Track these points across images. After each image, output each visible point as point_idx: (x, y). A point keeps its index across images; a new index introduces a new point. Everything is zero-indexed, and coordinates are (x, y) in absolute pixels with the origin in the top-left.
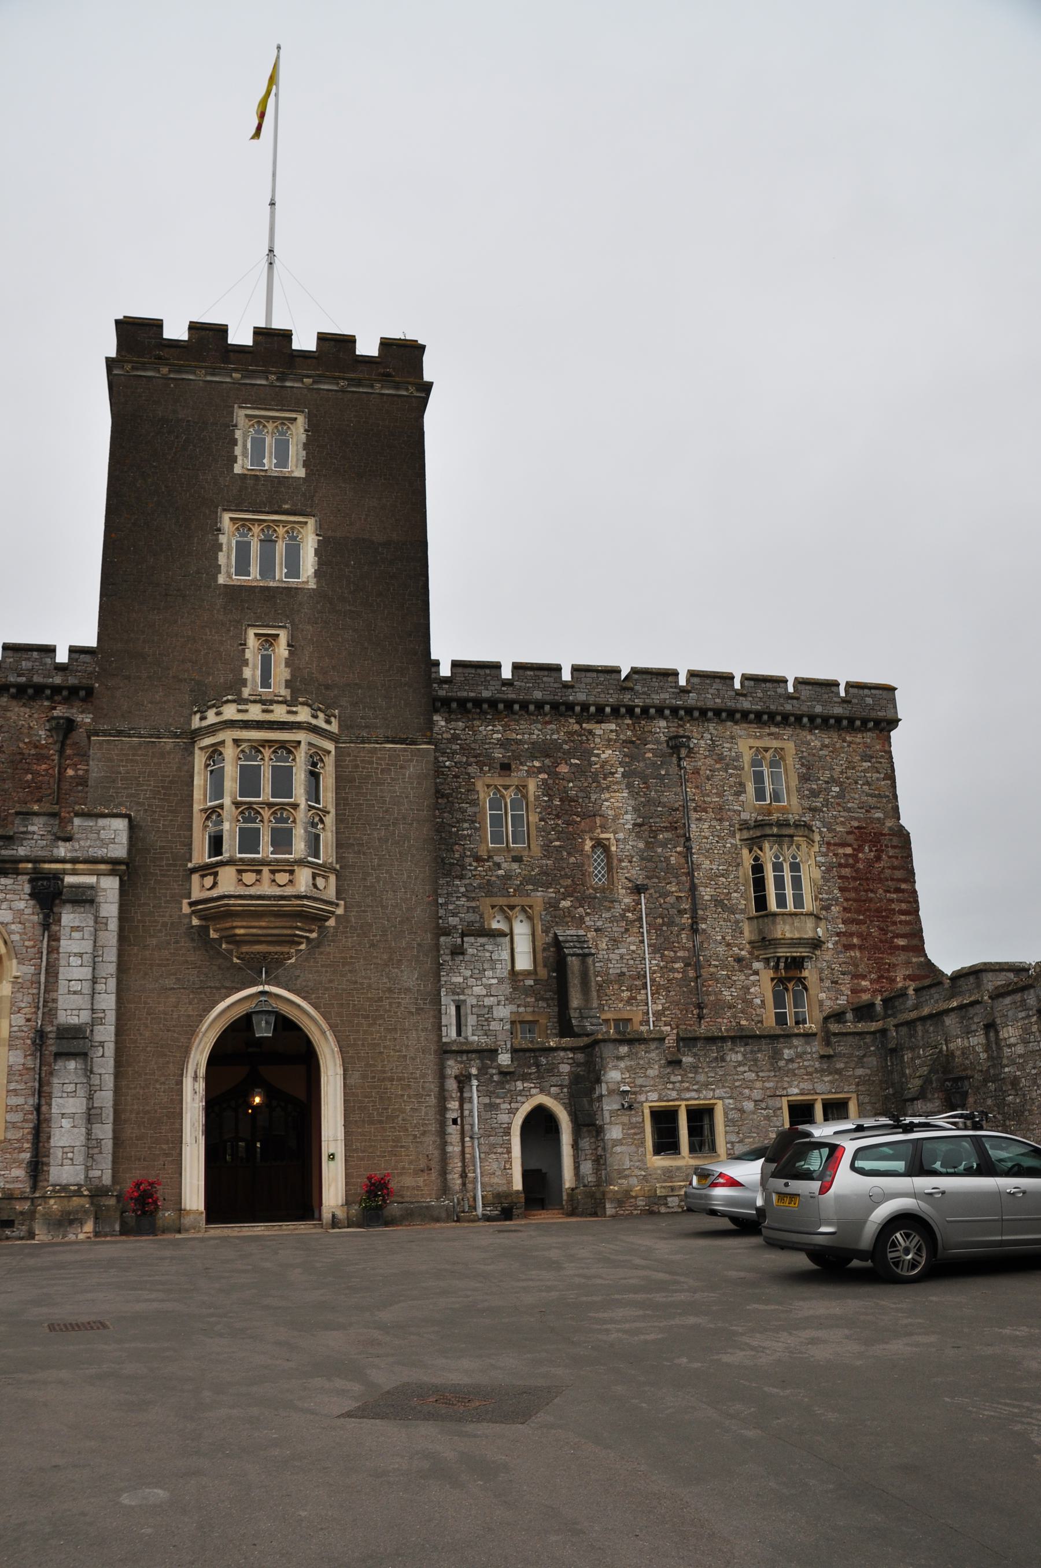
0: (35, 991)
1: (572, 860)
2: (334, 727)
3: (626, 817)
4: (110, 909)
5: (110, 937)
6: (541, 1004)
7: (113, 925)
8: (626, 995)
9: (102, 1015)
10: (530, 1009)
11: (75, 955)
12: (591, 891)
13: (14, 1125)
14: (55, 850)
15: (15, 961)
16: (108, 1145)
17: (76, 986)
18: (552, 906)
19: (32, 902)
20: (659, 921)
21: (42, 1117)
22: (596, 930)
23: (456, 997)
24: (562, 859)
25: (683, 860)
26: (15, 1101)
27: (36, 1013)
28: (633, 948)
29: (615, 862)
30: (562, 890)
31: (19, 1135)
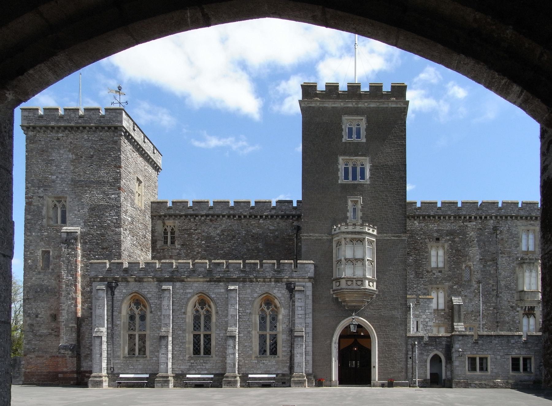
0: (289, 318)
1: (458, 272)
2: (375, 233)
3: (477, 256)
4: (309, 293)
5: (310, 301)
6: (446, 320)
7: (311, 297)
8: (473, 318)
9: (308, 325)
10: (442, 322)
11: (300, 307)
12: (464, 282)
13: (285, 356)
14: (292, 275)
15: (283, 308)
16: (311, 362)
17: (300, 316)
18: (451, 287)
19: (287, 291)
20: (486, 293)
21: (292, 354)
22: (465, 296)
23: (417, 318)
24: (455, 272)
25: (495, 272)
26: (284, 349)
27: (289, 324)
28: (477, 302)
29: (472, 272)
30: (454, 282)
31: (286, 359)
